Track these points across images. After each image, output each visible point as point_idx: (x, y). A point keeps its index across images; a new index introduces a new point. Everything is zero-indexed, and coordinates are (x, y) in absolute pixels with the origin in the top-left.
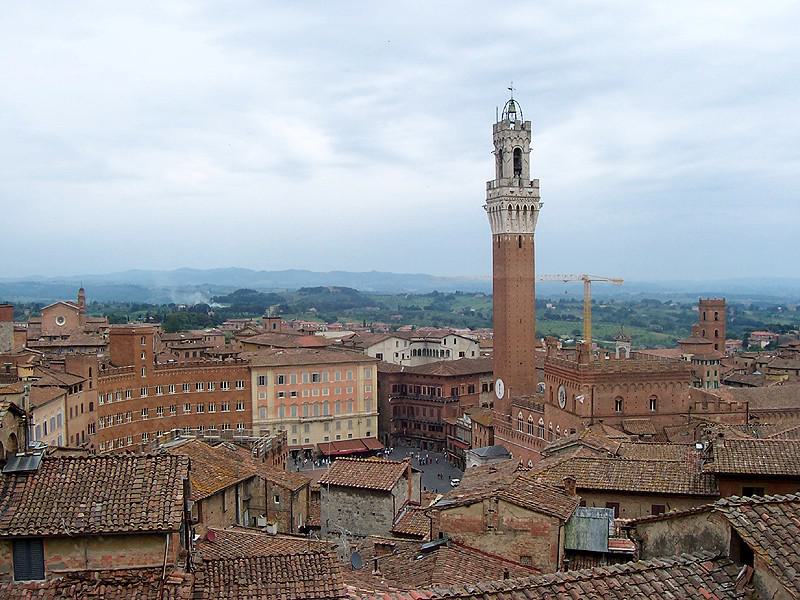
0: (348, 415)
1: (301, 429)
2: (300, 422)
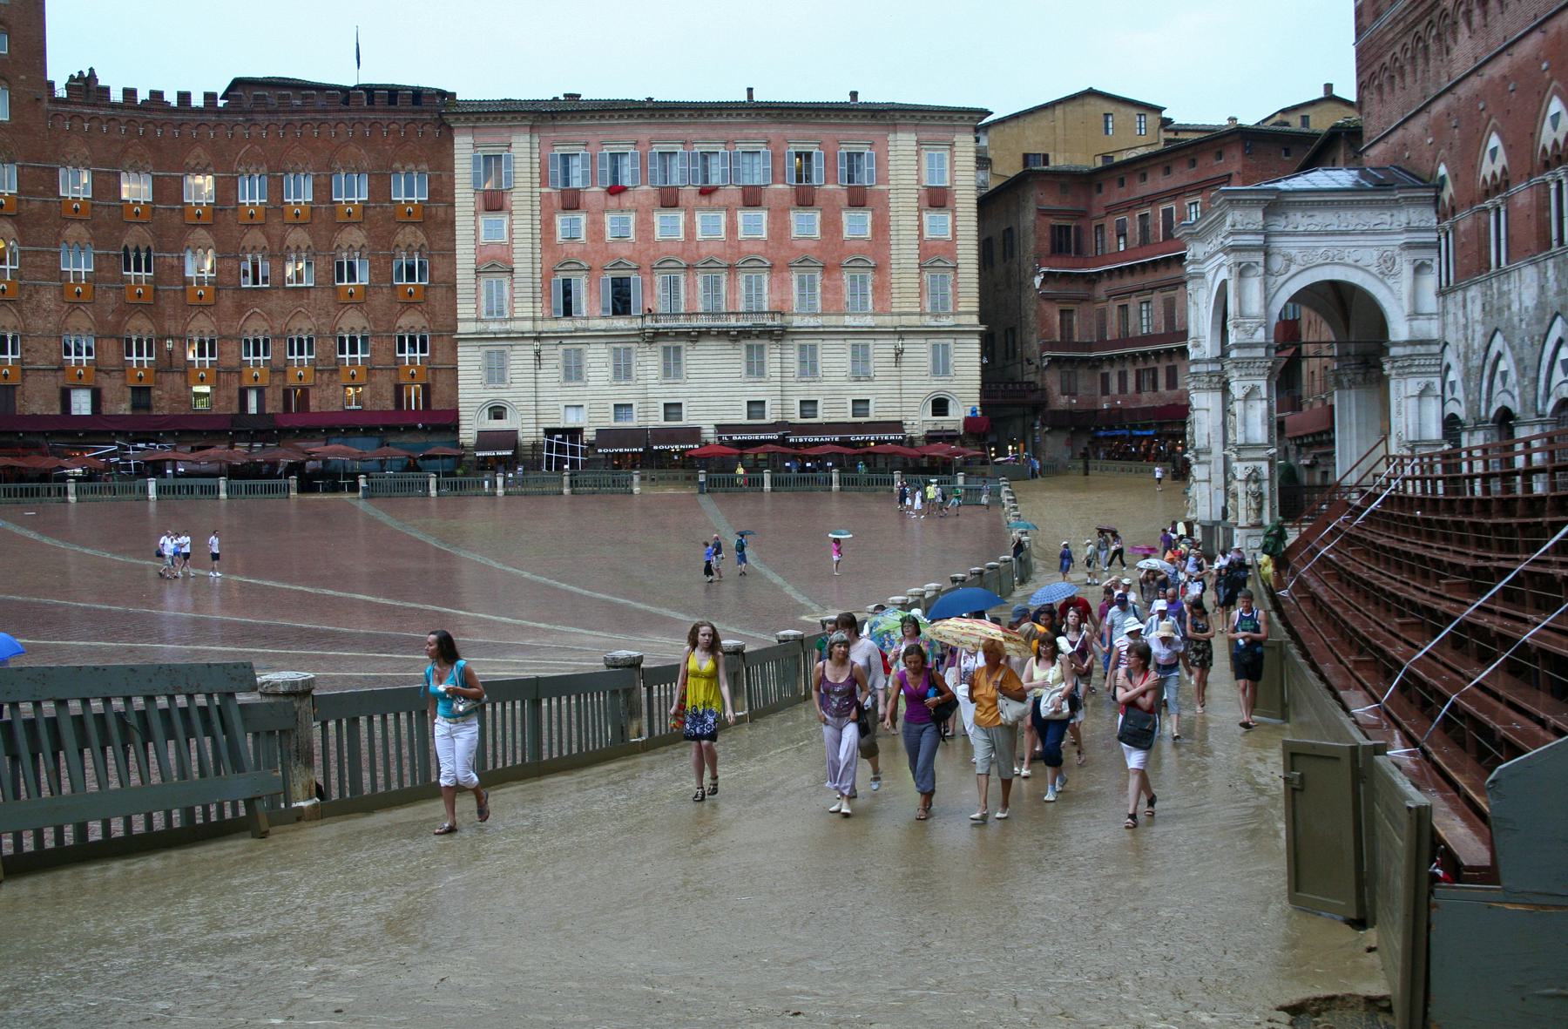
1: (649, 361)
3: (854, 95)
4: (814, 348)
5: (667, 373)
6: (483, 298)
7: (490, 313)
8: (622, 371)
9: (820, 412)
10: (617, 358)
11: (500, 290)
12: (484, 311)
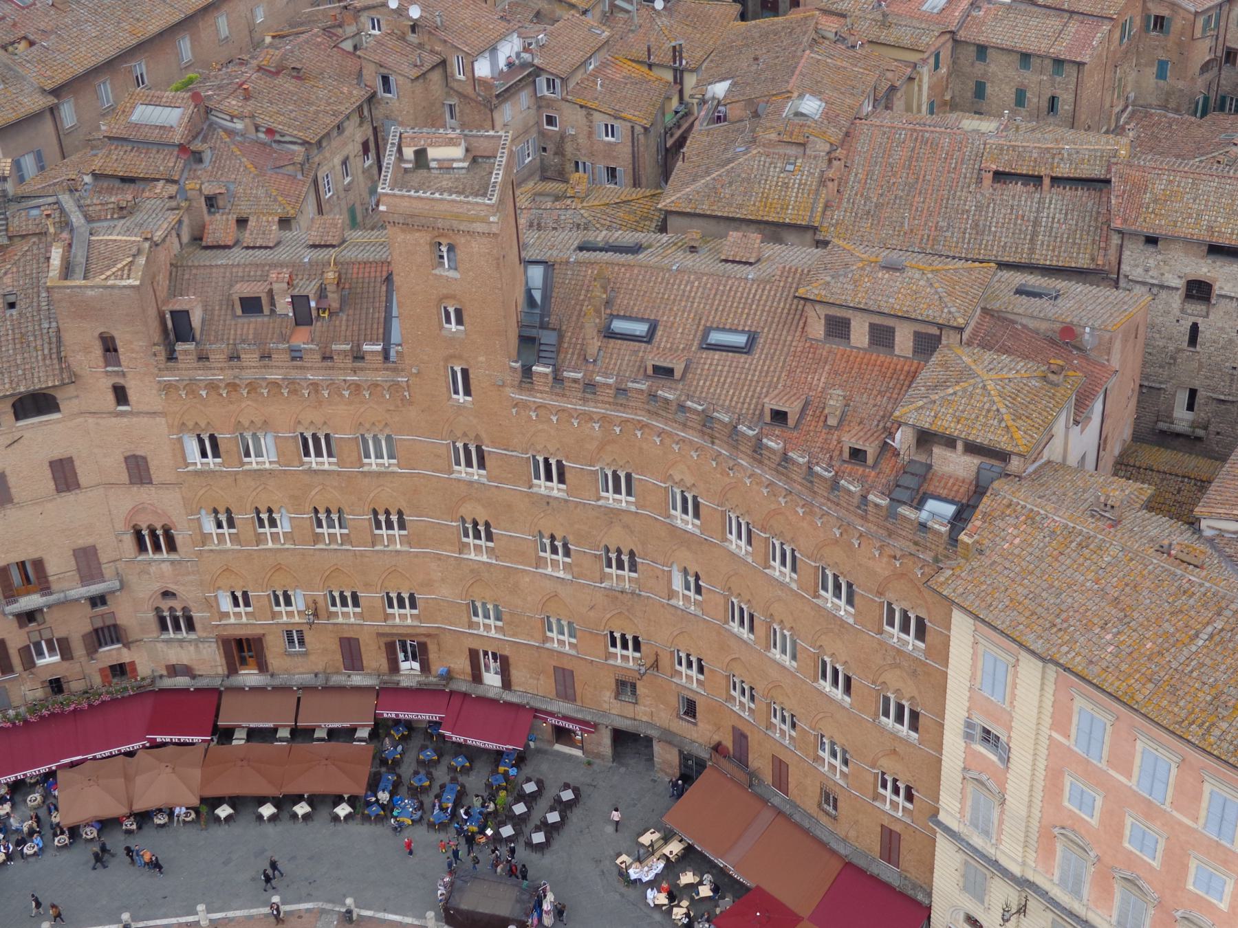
6: (969, 803)
12: (968, 816)
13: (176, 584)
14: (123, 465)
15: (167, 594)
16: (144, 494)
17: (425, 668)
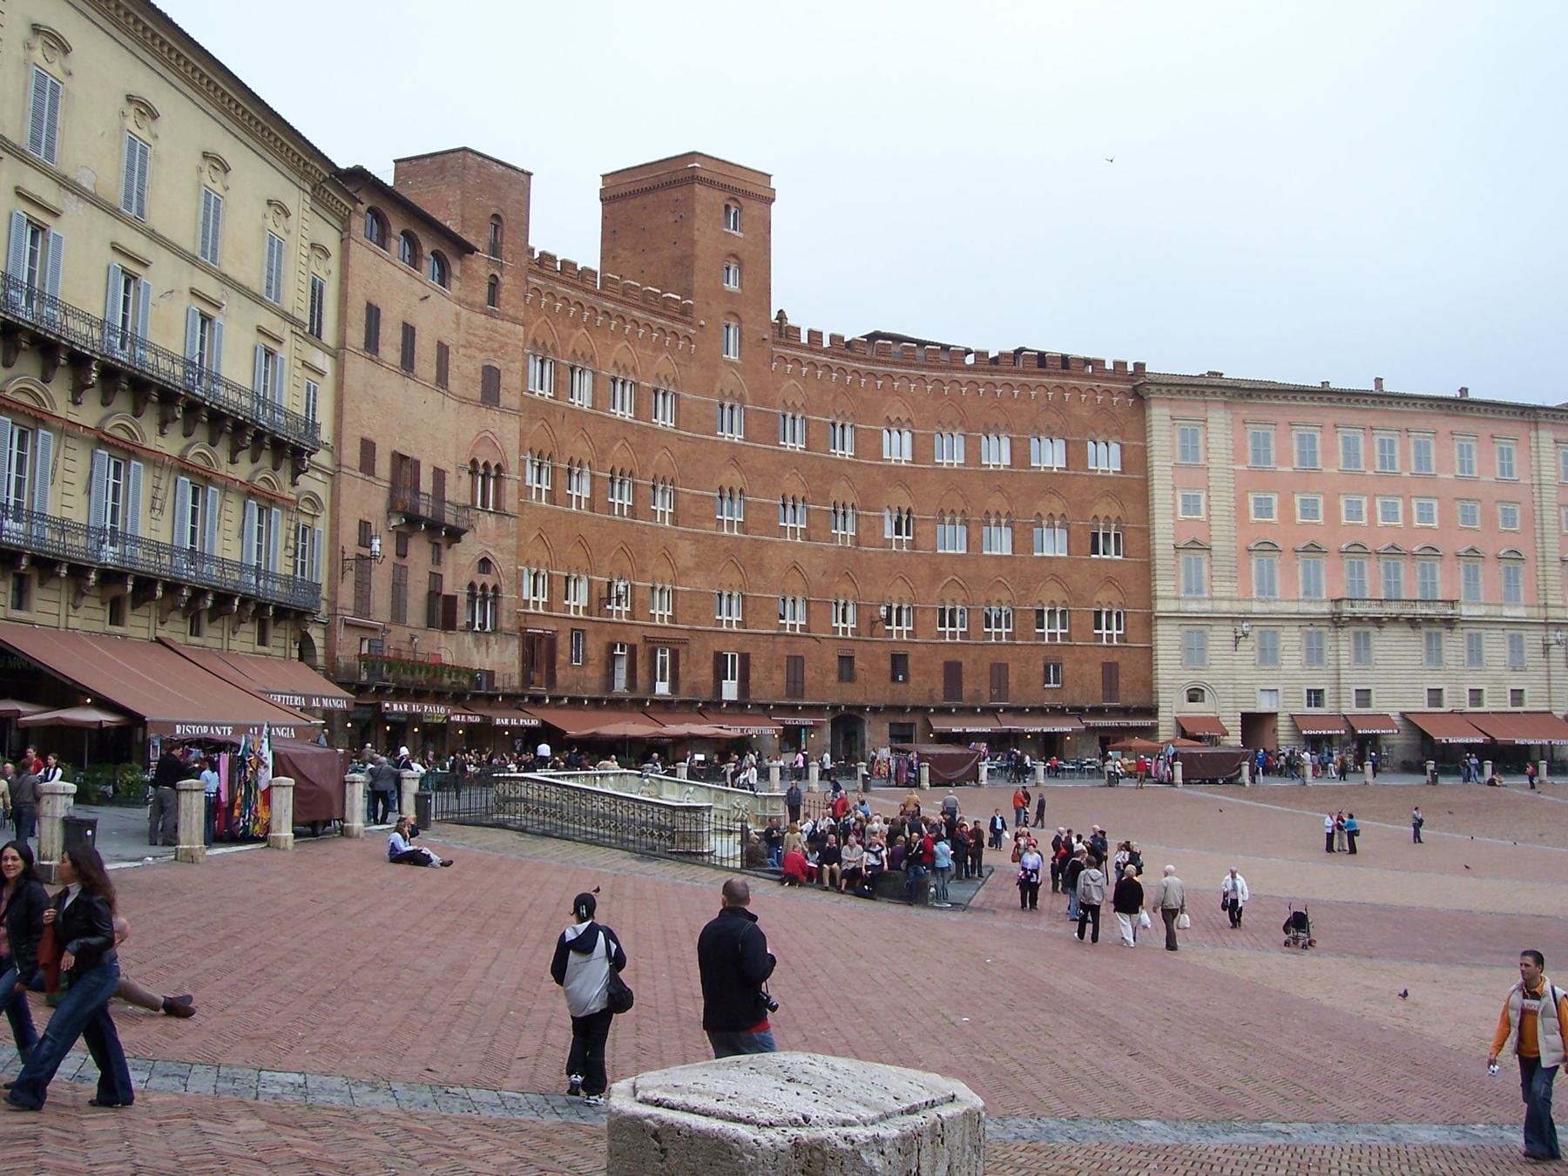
0: (1509, 612)
1: (1342, 645)
2: (1337, 621)
3: (1464, 391)
4: (1479, 636)
5: (1358, 659)
7: (1188, 590)
8: (1314, 656)
9: (1486, 700)
10: (1309, 643)
11: (1199, 567)
12: (1182, 588)
13: (495, 547)
14: (480, 377)
15: (485, 564)
16: (491, 418)
17: (674, 687)
